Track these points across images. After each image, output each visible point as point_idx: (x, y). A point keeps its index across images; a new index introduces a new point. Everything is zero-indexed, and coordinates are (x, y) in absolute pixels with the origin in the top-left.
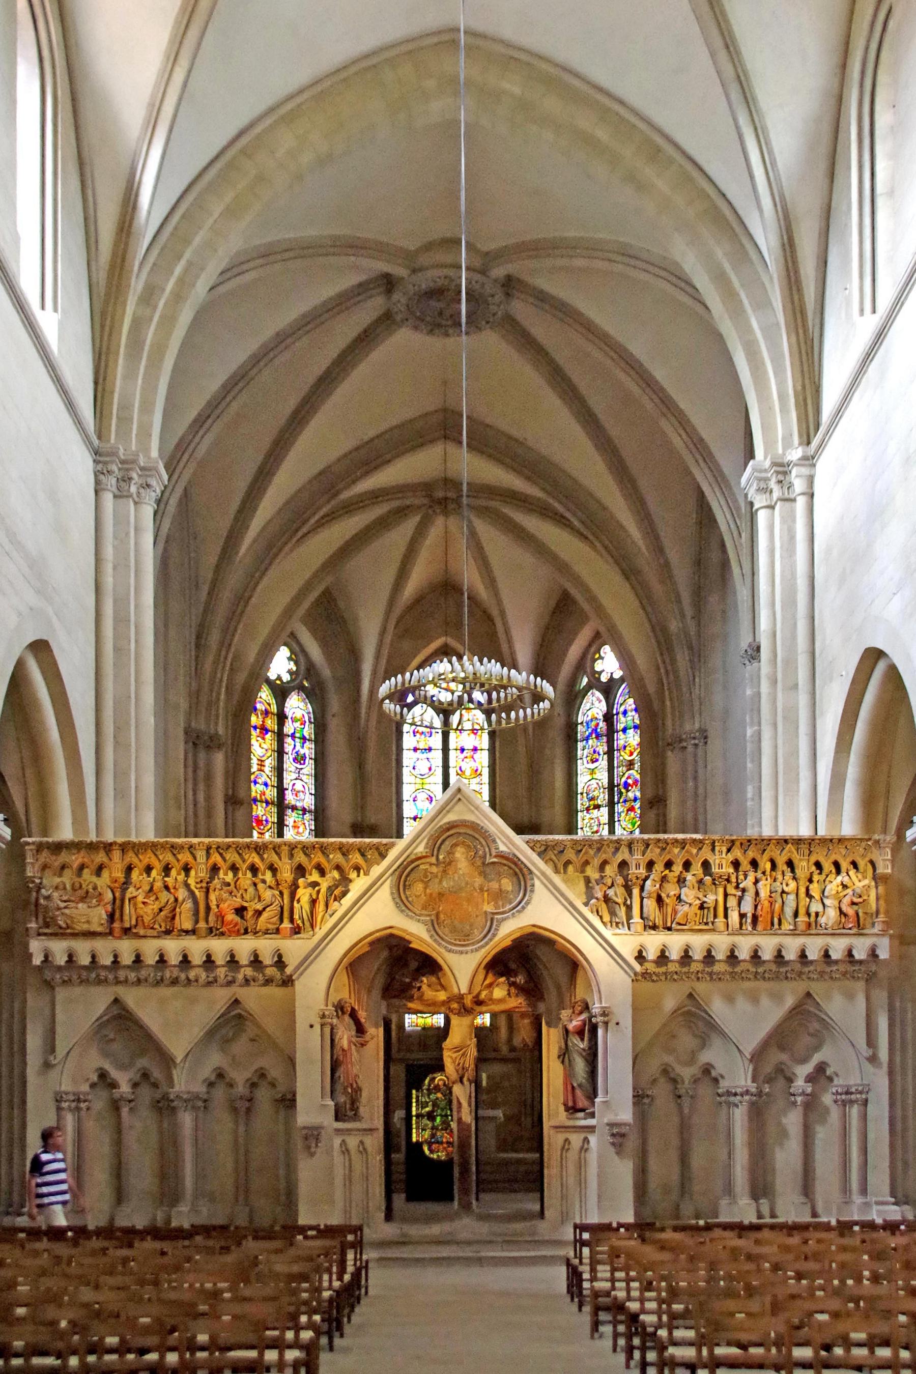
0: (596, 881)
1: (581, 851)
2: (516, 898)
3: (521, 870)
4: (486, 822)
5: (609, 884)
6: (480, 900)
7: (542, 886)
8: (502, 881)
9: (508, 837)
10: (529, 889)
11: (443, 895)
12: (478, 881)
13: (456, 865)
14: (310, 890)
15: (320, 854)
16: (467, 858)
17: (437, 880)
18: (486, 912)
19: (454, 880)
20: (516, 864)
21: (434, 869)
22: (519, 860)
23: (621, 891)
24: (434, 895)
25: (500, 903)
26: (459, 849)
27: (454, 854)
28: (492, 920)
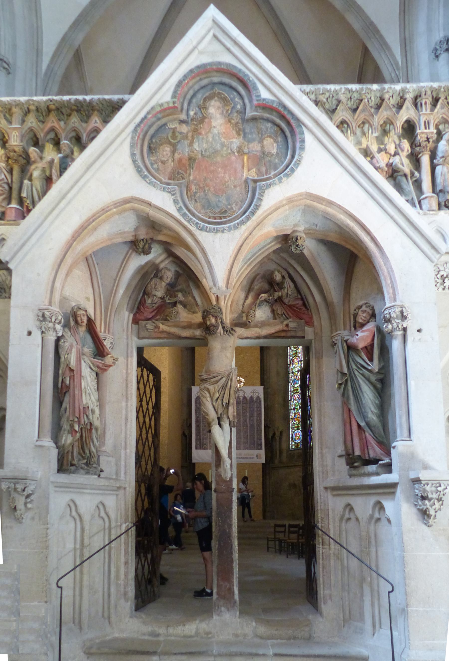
2: (283, 163)
3: (288, 123)
6: (239, 167)
7: (316, 143)
8: (265, 142)
11: (195, 160)
12: (236, 142)
13: (210, 122)
16: (222, 113)
17: (186, 142)
18: (246, 181)
19: (207, 142)
20: (283, 117)
21: (184, 129)
24: (184, 161)
26: (213, 102)
27: (205, 108)
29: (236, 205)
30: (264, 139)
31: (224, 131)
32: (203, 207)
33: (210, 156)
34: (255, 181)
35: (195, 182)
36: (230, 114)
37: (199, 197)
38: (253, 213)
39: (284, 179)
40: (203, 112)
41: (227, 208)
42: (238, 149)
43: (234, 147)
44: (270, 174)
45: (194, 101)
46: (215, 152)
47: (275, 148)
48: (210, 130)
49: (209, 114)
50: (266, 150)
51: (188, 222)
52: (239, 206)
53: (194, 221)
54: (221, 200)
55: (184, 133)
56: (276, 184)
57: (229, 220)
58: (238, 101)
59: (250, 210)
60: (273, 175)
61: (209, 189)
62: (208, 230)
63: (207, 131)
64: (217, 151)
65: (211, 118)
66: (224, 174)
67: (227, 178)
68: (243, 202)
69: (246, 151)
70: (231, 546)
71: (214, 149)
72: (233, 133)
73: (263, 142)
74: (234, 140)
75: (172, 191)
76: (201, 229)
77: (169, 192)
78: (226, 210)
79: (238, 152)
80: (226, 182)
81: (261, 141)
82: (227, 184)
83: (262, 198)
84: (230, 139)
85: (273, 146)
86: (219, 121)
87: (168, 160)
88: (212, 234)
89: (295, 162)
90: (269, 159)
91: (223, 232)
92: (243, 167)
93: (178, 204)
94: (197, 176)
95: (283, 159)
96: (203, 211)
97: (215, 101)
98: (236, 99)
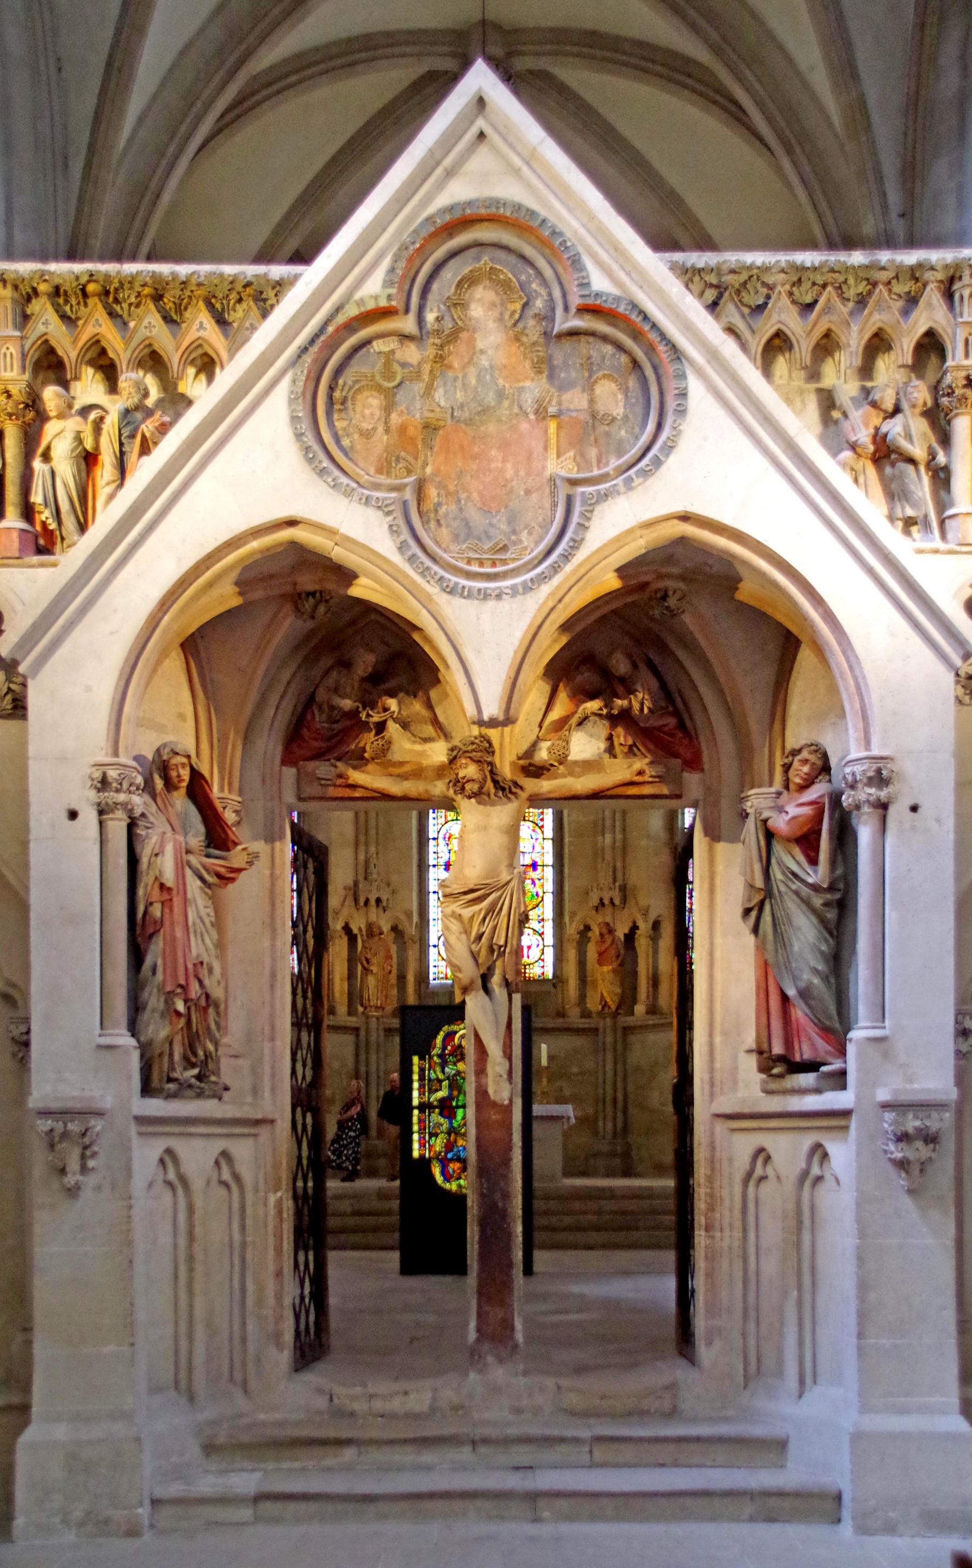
0: (852, 399)
1: (810, 306)
3: (650, 350)
4: (557, 205)
5: (889, 405)
6: (538, 447)
7: (710, 399)
8: (599, 390)
9: (617, 249)
10: (671, 404)
13: (471, 342)
14: (73, 424)
15: (100, 314)
16: (501, 319)
17: (419, 387)
18: (552, 480)
19: (465, 386)
21: (412, 353)
22: (646, 317)
23: (920, 426)
24: (411, 431)
25: (593, 453)
28: (569, 501)
29: (530, 533)
30: (596, 382)
31: (504, 361)
32: (456, 537)
33: (471, 420)
34: (574, 482)
35: (437, 479)
36: (518, 321)
37: (446, 515)
38: (566, 557)
39: (637, 481)
40: (455, 317)
41: (509, 539)
42: (536, 406)
43: (526, 401)
44: (607, 464)
45: (435, 286)
46: (484, 411)
47: (621, 404)
48: (472, 359)
49: (470, 319)
50: (601, 407)
51: (422, 574)
52: (535, 536)
53: (436, 573)
54: (495, 521)
55: (412, 366)
56: (618, 493)
57: (513, 570)
58: (538, 289)
59: (559, 550)
60: (615, 469)
61: (469, 497)
62: (466, 593)
63: (466, 360)
64: (488, 408)
65: (475, 330)
66: (504, 460)
67: (510, 473)
68: (545, 527)
69: (552, 410)
70: (508, 1235)
71: (480, 405)
72: (524, 367)
73: (593, 390)
74: (528, 384)
75: (386, 506)
76: (452, 591)
77: (379, 508)
78: (505, 546)
79: (537, 412)
80: (507, 480)
81: (589, 387)
82: (509, 486)
83: (586, 524)
84: (519, 381)
85: (616, 402)
86: (493, 338)
87: (374, 429)
88: (476, 602)
89: (665, 443)
90: (607, 428)
91: (499, 597)
92: (546, 448)
93: (398, 536)
94: (442, 468)
95: (637, 430)
96: (455, 547)
97: (485, 288)
98: (534, 286)
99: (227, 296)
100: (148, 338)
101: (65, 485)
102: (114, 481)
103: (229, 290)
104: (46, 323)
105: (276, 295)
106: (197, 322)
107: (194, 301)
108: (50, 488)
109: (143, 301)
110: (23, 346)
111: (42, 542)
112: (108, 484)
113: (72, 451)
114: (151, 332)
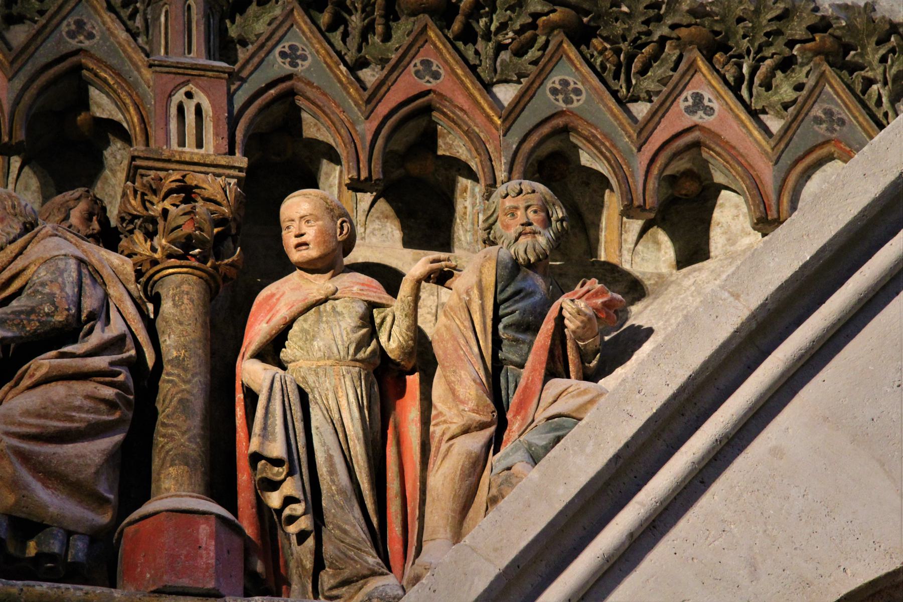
99: (760, 49)
100: (561, 113)
101: (338, 429)
102: (482, 426)
103: (768, 35)
104: (292, 56)
105: (883, 60)
106: (688, 93)
107: (671, 52)
108: (299, 426)
109: (542, 39)
110: (230, 97)
111: (259, 567)
112: (466, 431)
113: (361, 345)
114: (568, 101)
